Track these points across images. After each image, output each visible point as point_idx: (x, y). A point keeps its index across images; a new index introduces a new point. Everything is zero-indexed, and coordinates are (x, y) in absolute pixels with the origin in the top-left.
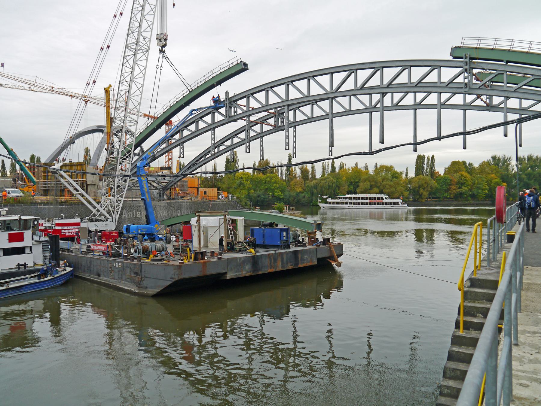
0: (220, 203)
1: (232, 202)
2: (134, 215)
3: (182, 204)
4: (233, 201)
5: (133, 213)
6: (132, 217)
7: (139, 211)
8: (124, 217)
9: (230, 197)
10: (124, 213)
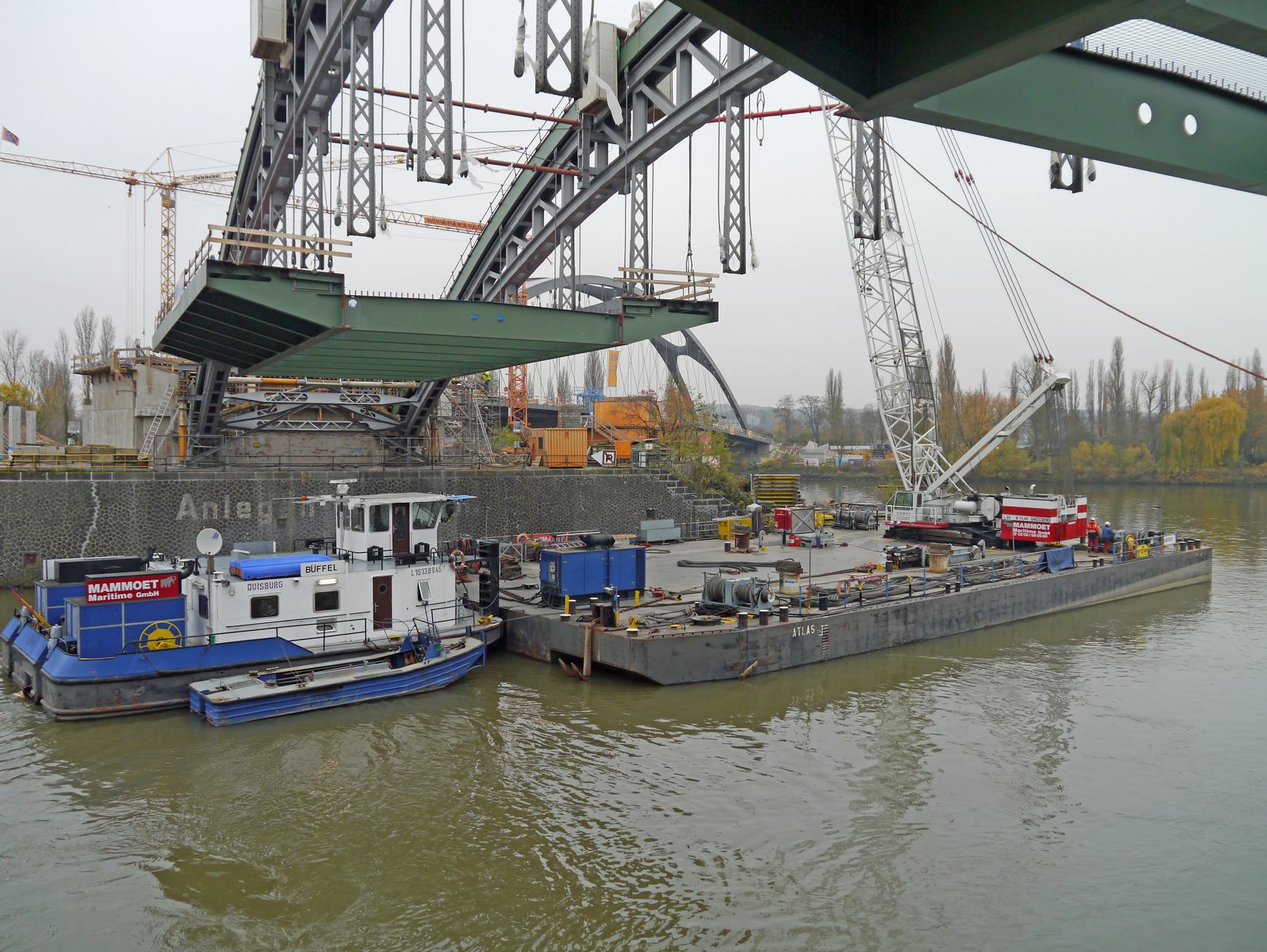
0: (593, 476)
1: (648, 476)
2: (227, 511)
3: (428, 478)
4: (653, 472)
5: (223, 504)
6: (215, 516)
7: (247, 500)
8: (185, 517)
9: (644, 459)
10: (183, 504)
